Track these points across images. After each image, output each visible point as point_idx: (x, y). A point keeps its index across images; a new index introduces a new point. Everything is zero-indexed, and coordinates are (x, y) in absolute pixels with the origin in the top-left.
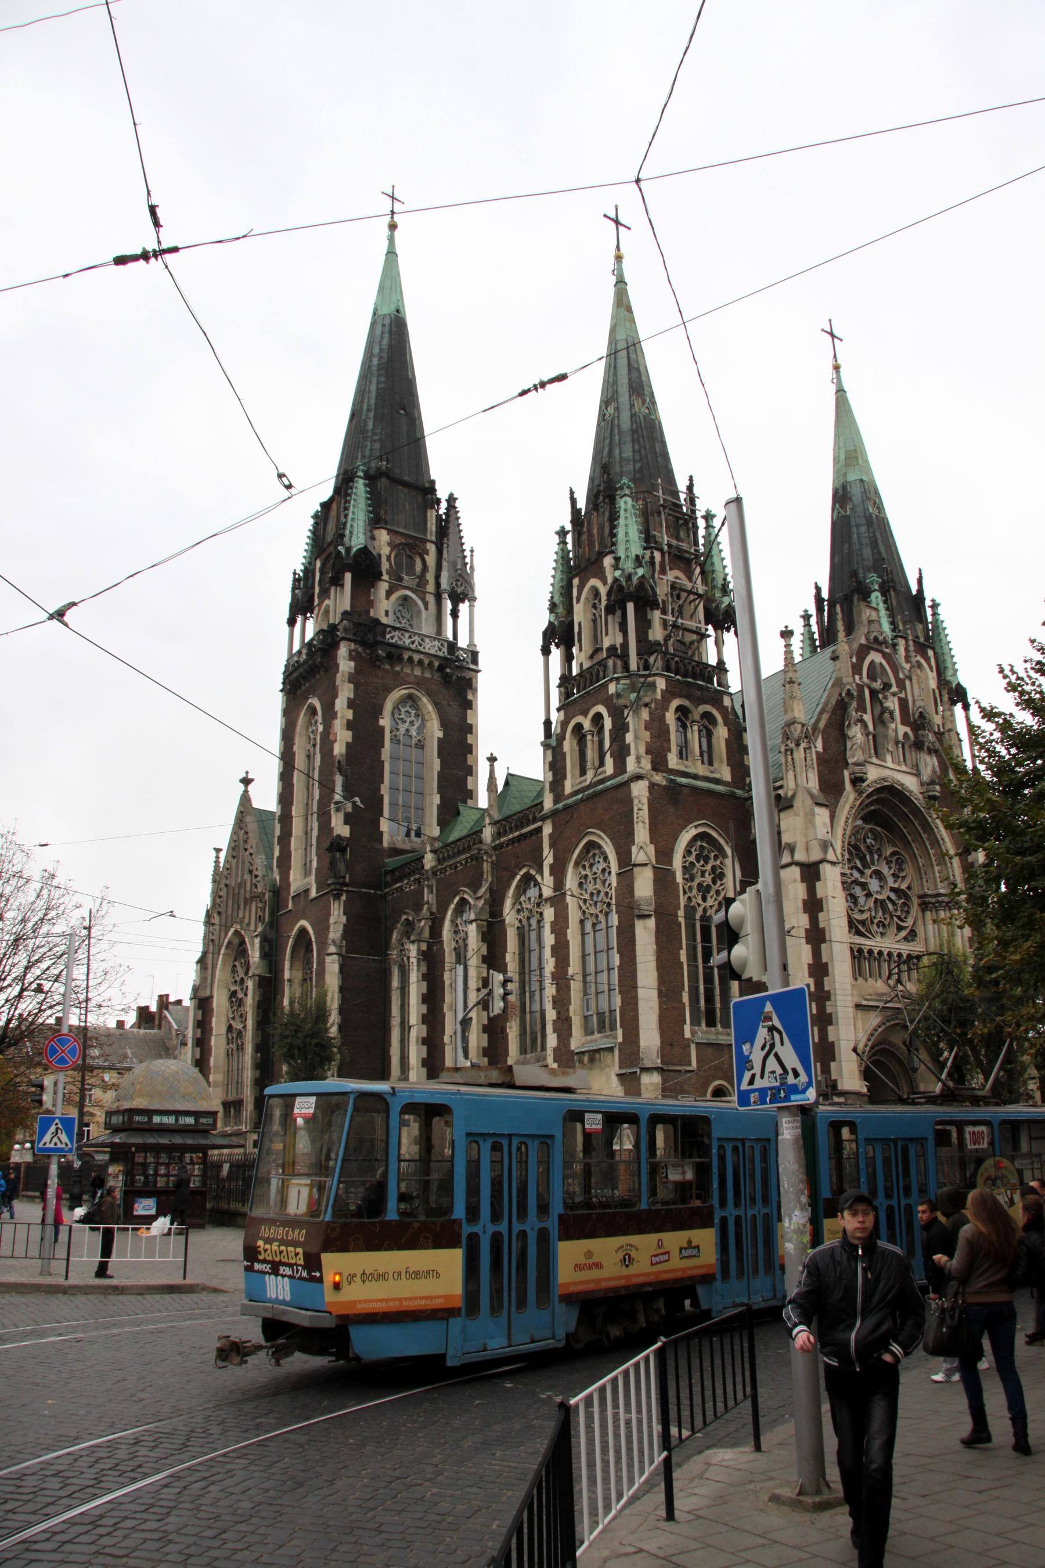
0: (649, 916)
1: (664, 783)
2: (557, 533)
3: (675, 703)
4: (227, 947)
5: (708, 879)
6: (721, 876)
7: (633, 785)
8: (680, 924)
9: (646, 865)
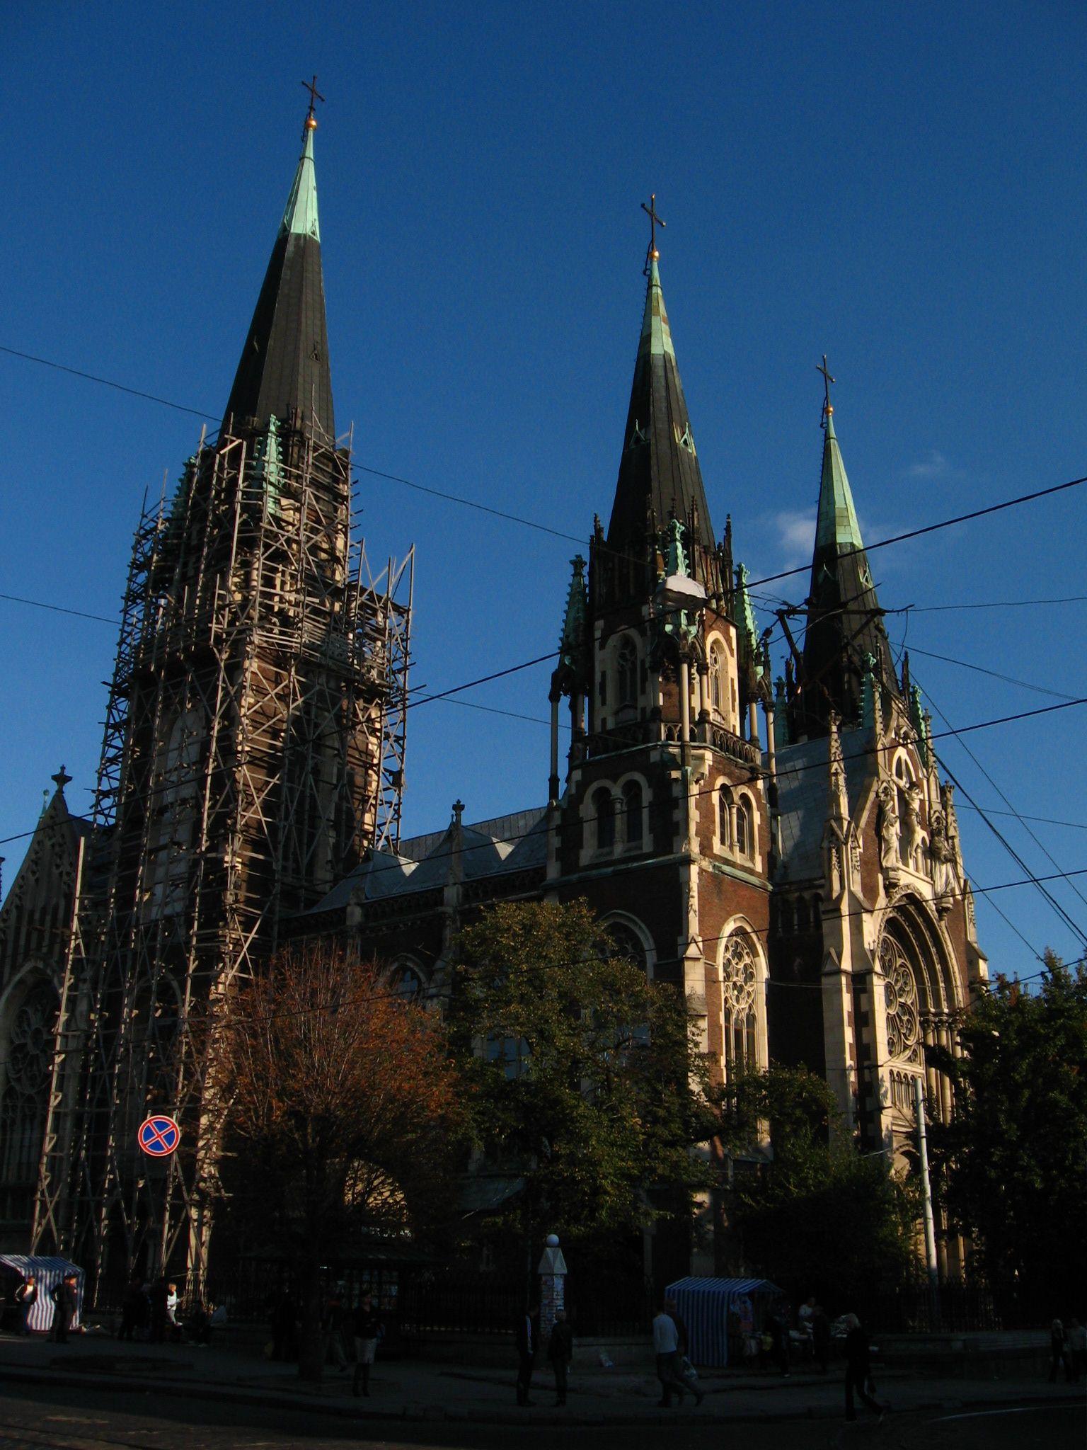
0: (704, 1016)
1: (711, 869)
2: (572, 563)
3: (721, 780)
4: (15, 987)
5: (739, 979)
6: (752, 975)
7: (681, 869)
8: (721, 1027)
9: (699, 959)
